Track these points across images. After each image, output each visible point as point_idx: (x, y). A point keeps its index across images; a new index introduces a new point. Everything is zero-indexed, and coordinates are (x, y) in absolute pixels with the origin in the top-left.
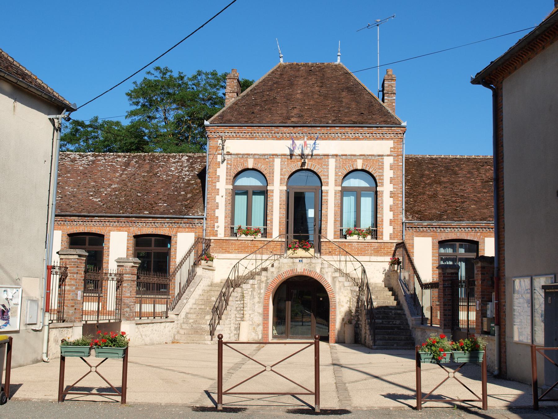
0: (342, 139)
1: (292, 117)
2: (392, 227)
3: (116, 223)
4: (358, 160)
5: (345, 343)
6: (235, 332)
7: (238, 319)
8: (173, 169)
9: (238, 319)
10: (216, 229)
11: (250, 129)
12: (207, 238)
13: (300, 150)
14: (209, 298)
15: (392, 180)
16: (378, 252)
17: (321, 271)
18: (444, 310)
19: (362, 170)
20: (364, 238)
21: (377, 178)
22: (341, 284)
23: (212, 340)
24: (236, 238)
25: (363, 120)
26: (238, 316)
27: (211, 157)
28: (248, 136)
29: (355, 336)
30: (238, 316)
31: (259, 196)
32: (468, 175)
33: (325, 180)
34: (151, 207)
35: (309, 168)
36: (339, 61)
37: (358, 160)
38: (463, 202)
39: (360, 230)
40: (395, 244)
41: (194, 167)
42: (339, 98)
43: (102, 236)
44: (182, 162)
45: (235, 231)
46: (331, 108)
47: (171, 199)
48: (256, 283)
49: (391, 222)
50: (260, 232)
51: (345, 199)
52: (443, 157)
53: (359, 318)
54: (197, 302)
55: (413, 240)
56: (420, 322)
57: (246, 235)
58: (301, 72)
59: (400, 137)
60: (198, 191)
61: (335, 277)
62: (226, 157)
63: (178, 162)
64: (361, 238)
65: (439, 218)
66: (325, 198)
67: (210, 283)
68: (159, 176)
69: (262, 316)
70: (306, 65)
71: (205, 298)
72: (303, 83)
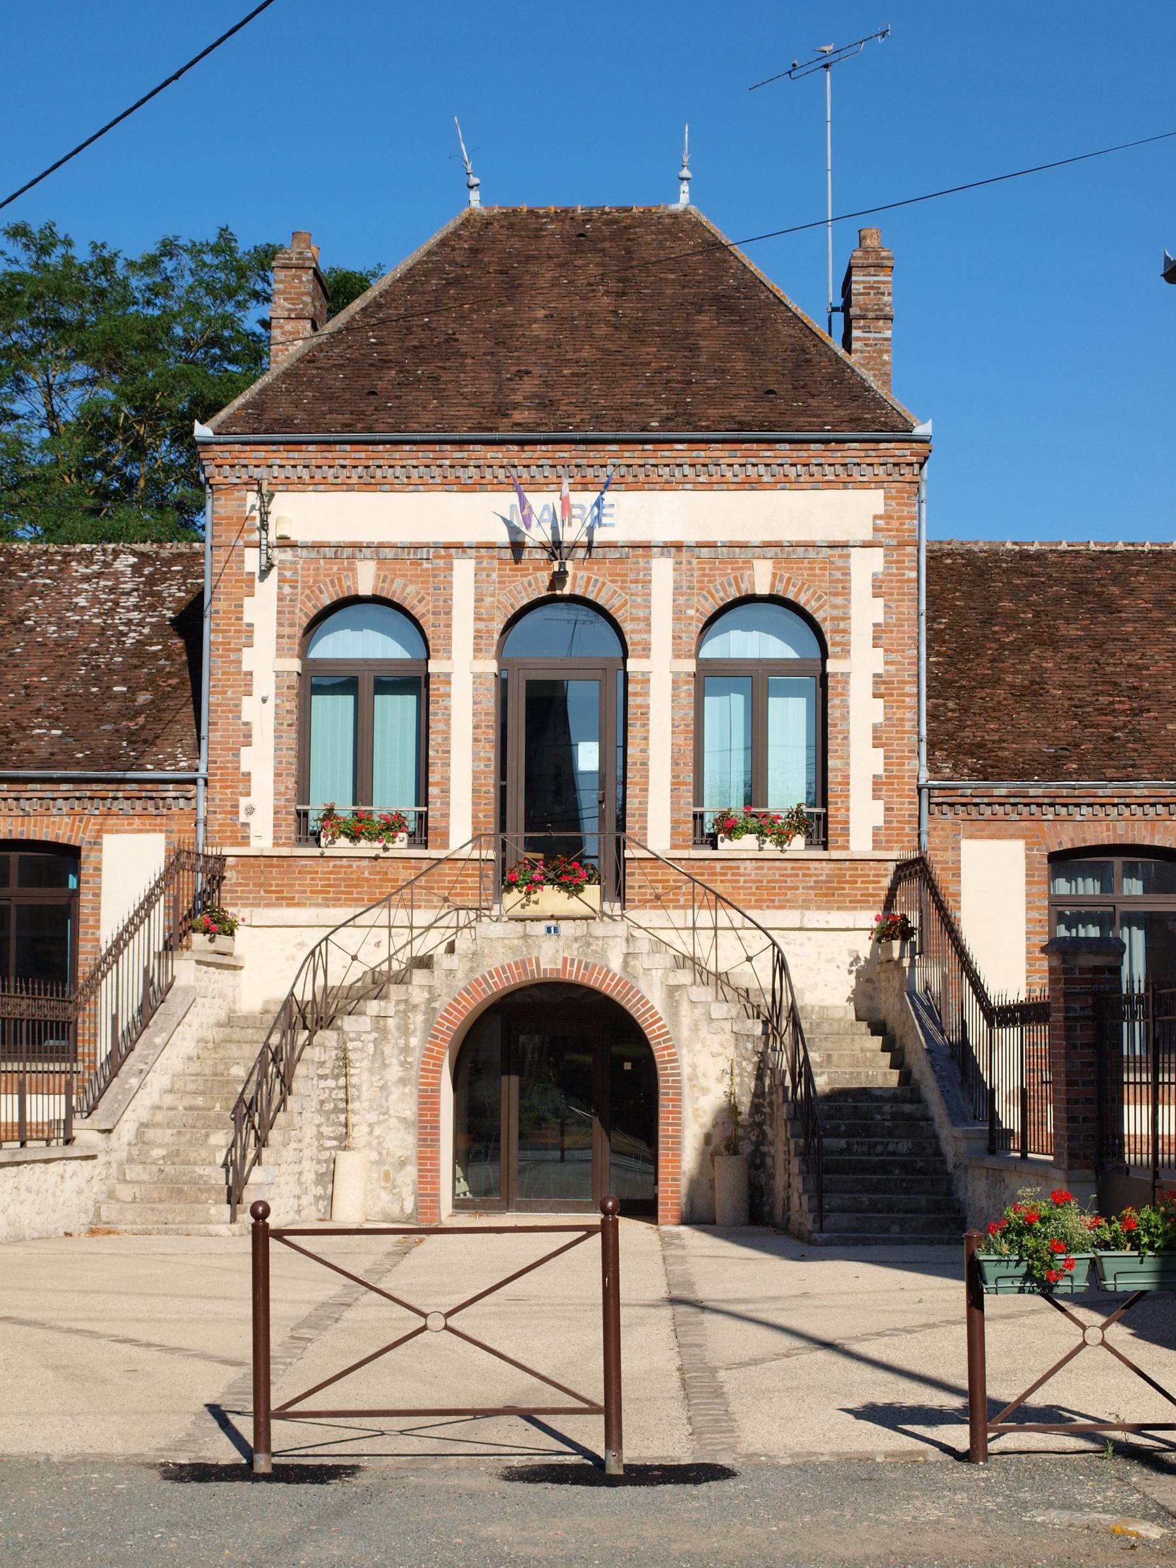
0: (698, 486)
1: (516, 406)
2: (880, 805)
4: (756, 563)
5: (714, 1223)
6: (319, 1191)
7: (329, 1143)
8: (81, 601)
9: (329, 1143)
10: (243, 818)
11: (361, 454)
12: (212, 851)
13: (547, 527)
14: (220, 1068)
15: (879, 635)
16: (830, 894)
17: (626, 964)
18: (1069, 1101)
19: (772, 599)
20: (781, 843)
21: (826, 627)
22: (700, 1010)
23: (233, 1219)
24: (316, 852)
25: (774, 417)
26: (327, 1130)
27: (222, 555)
28: (354, 480)
29: (751, 1197)
30: (327, 1130)
31: (398, 698)
32: (1156, 614)
33: (636, 637)
36: (684, 199)
37: (756, 563)
38: (1137, 712)
39: (765, 816)
40: (892, 867)
41: (158, 594)
42: (688, 334)
44: (117, 575)
45: (313, 825)
46: (658, 372)
48: (391, 1011)
49: (878, 786)
50: (402, 827)
51: (711, 704)
52: (1064, 547)
53: (763, 1134)
54: (179, 1084)
55: (957, 849)
56: (983, 1144)
57: (354, 837)
58: (547, 241)
59: (908, 477)
60: (174, 681)
61: (678, 987)
62: (278, 555)
63: (99, 575)
65: (1052, 769)
66: (639, 700)
67: (223, 1016)
68: (32, 629)
69: (414, 1131)
70: (564, 215)
71: (208, 1071)
72: (555, 283)
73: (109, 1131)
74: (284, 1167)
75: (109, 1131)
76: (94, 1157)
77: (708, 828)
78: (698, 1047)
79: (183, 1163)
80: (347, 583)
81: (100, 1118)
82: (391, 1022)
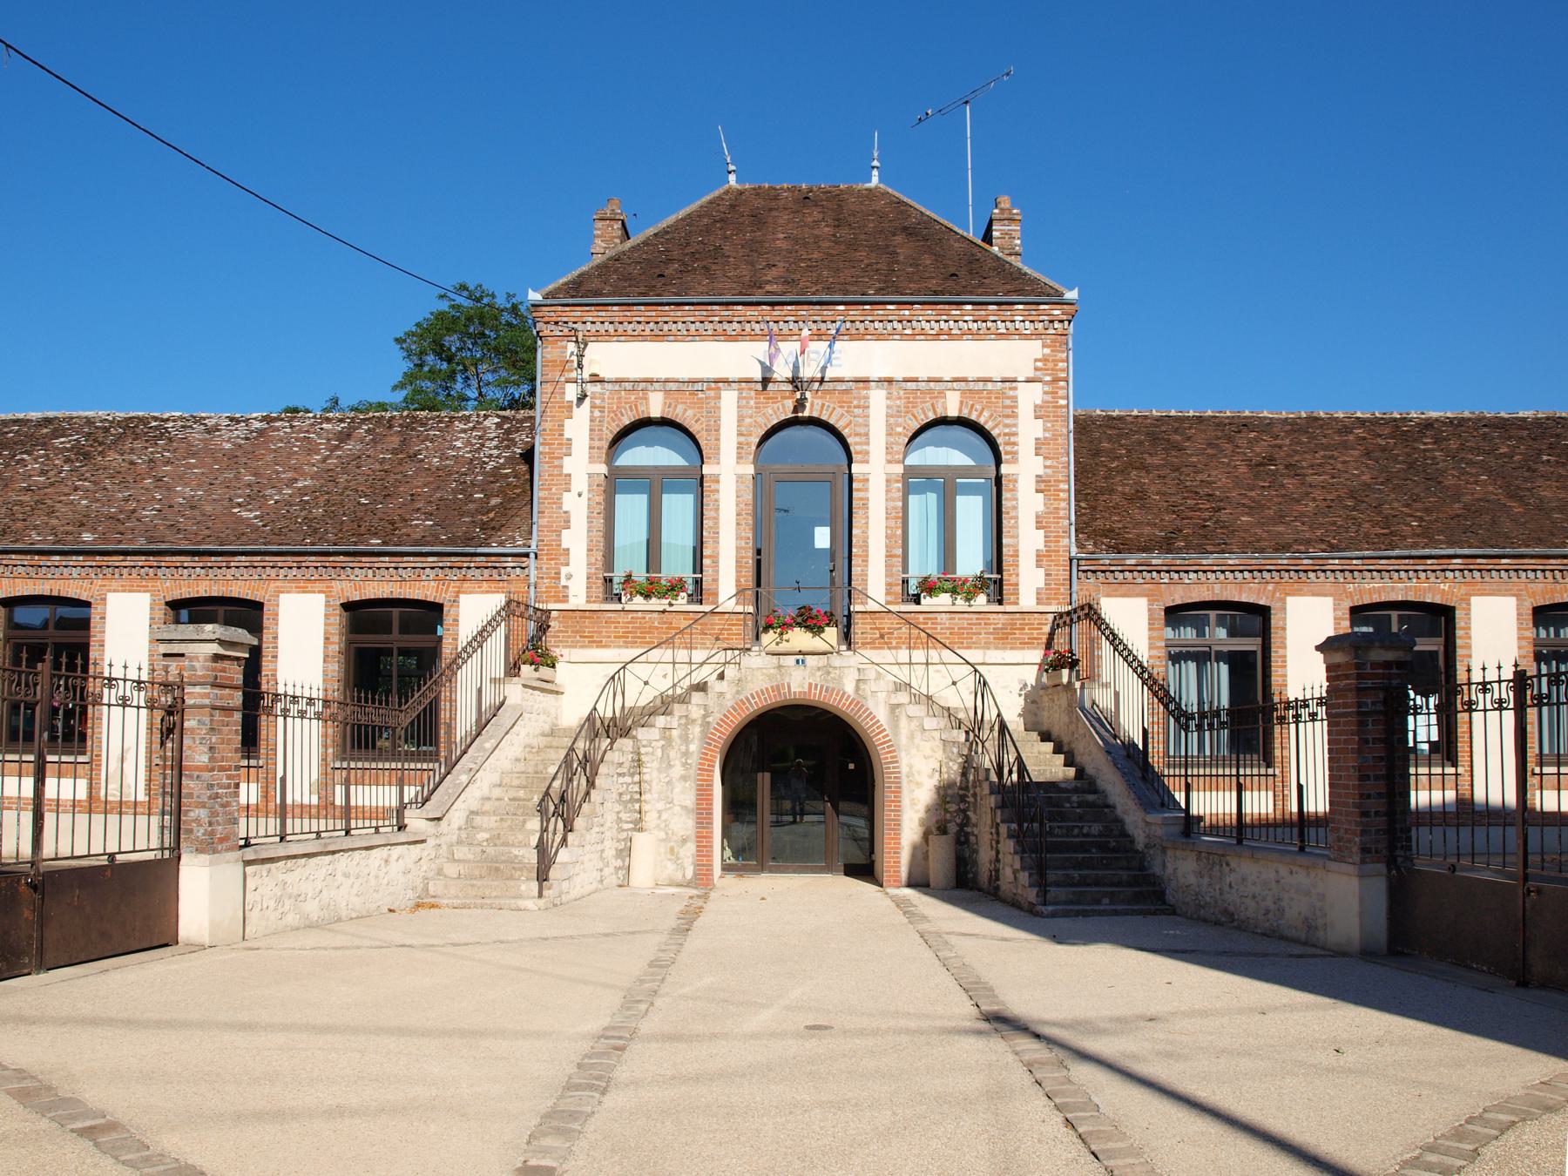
3: (294, 571)
5: (928, 886)
6: (619, 863)
7: (626, 826)
8: (459, 444)
9: (626, 826)
10: (563, 582)
14: (540, 768)
16: (1004, 638)
17: (857, 688)
22: (915, 723)
24: (619, 607)
26: (624, 816)
27: (549, 388)
31: (680, 496)
33: (858, 448)
34: (390, 530)
35: (815, 414)
43: (258, 606)
44: (485, 429)
45: (617, 589)
47: (444, 511)
50: (683, 589)
53: (967, 817)
54: (506, 780)
57: (647, 596)
61: (898, 705)
62: (590, 388)
64: (960, 601)
66: (861, 494)
67: (547, 728)
73: (439, 819)
74: (588, 847)
75: (439, 819)
76: (423, 841)
77: (913, 590)
78: (914, 751)
79: (503, 844)
80: (641, 408)
81: (431, 809)
82: (675, 733)
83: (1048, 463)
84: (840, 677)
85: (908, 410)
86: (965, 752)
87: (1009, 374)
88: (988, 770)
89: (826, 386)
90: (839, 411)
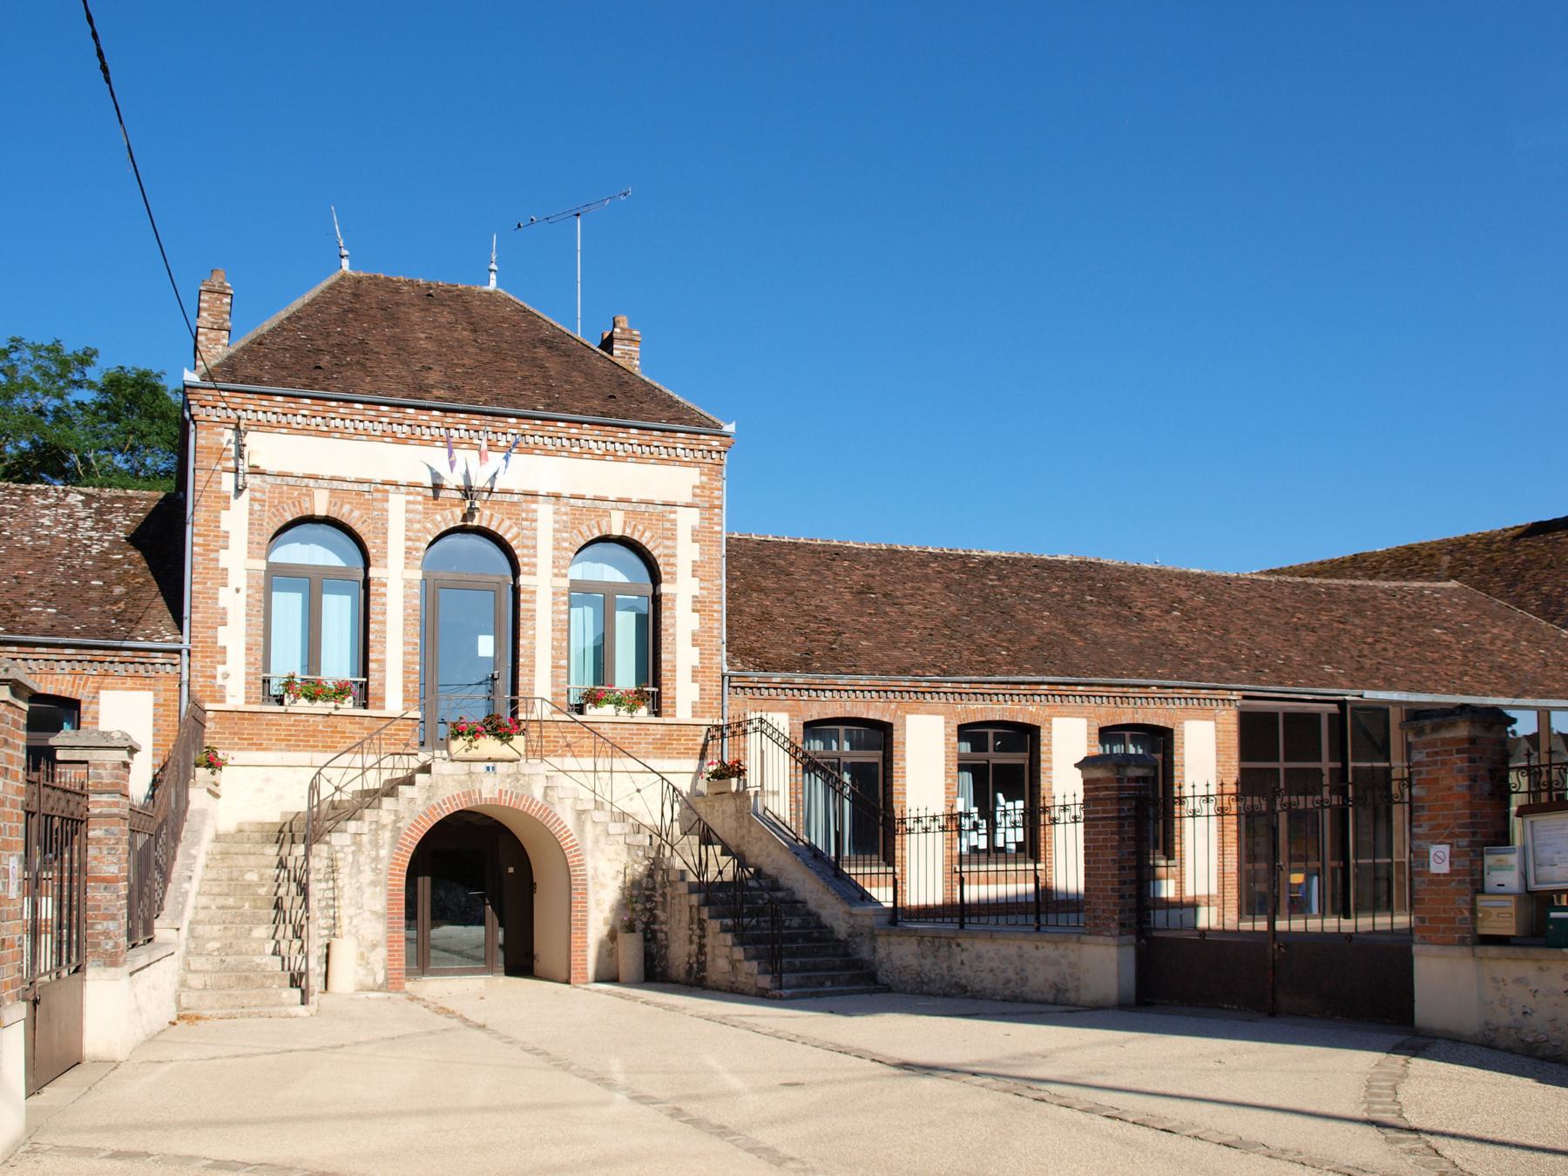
10: (219, 681)
17: (545, 795)
22: (600, 828)
24: (281, 709)
33: (525, 560)
35: (484, 524)
44: (70, 506)
45: (276, 689)
50: (350, 693)
56: (885, 919)
57: (312, 699)
60: (141, 580)
61: (584, 811)
68: (9, 538)
83: (705, 584)
84: (529, 784)
85: (574, 526)
86: (653, 855)
87: (671, 499)
88: (683, 872)
89: (494, 497)
90: (507, 523)
